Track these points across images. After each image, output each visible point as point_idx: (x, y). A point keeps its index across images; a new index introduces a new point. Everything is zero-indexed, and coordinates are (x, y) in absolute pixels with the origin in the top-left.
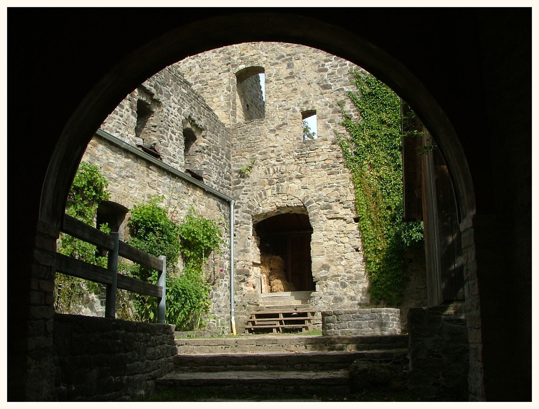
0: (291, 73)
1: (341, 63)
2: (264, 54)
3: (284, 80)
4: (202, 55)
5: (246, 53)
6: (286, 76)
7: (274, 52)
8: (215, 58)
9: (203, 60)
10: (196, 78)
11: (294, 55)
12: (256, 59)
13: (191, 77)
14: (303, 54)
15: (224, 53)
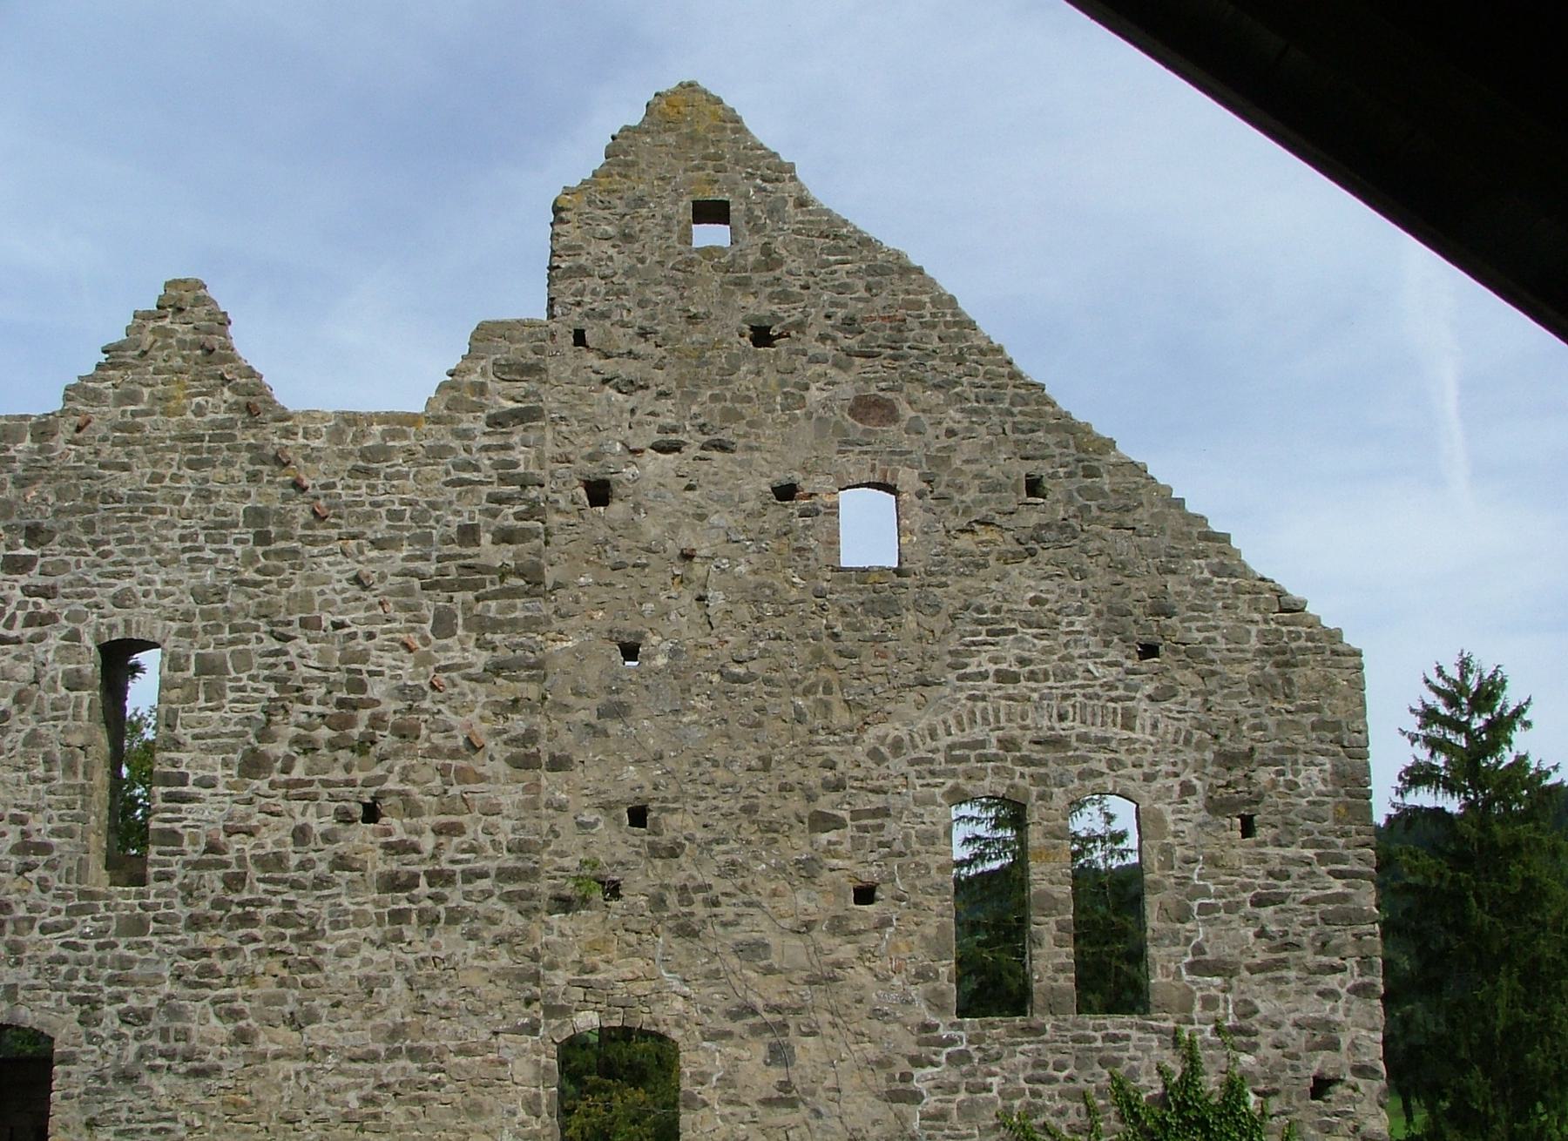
0: (785, 1086)
1: (971, 1080)
2: (676, 983)
3: (756, 1108)
4: (418, 938)
5: (602, 966)
6: (763, 1095)
7: (716, 985)
8: (476, 963)
9: (423, 960)
10: (396, 1032)
11: (797, 1011)
12: (643, 1000)
13: (371, 1023)
14: (828, 1016)
15: (512, 952)
